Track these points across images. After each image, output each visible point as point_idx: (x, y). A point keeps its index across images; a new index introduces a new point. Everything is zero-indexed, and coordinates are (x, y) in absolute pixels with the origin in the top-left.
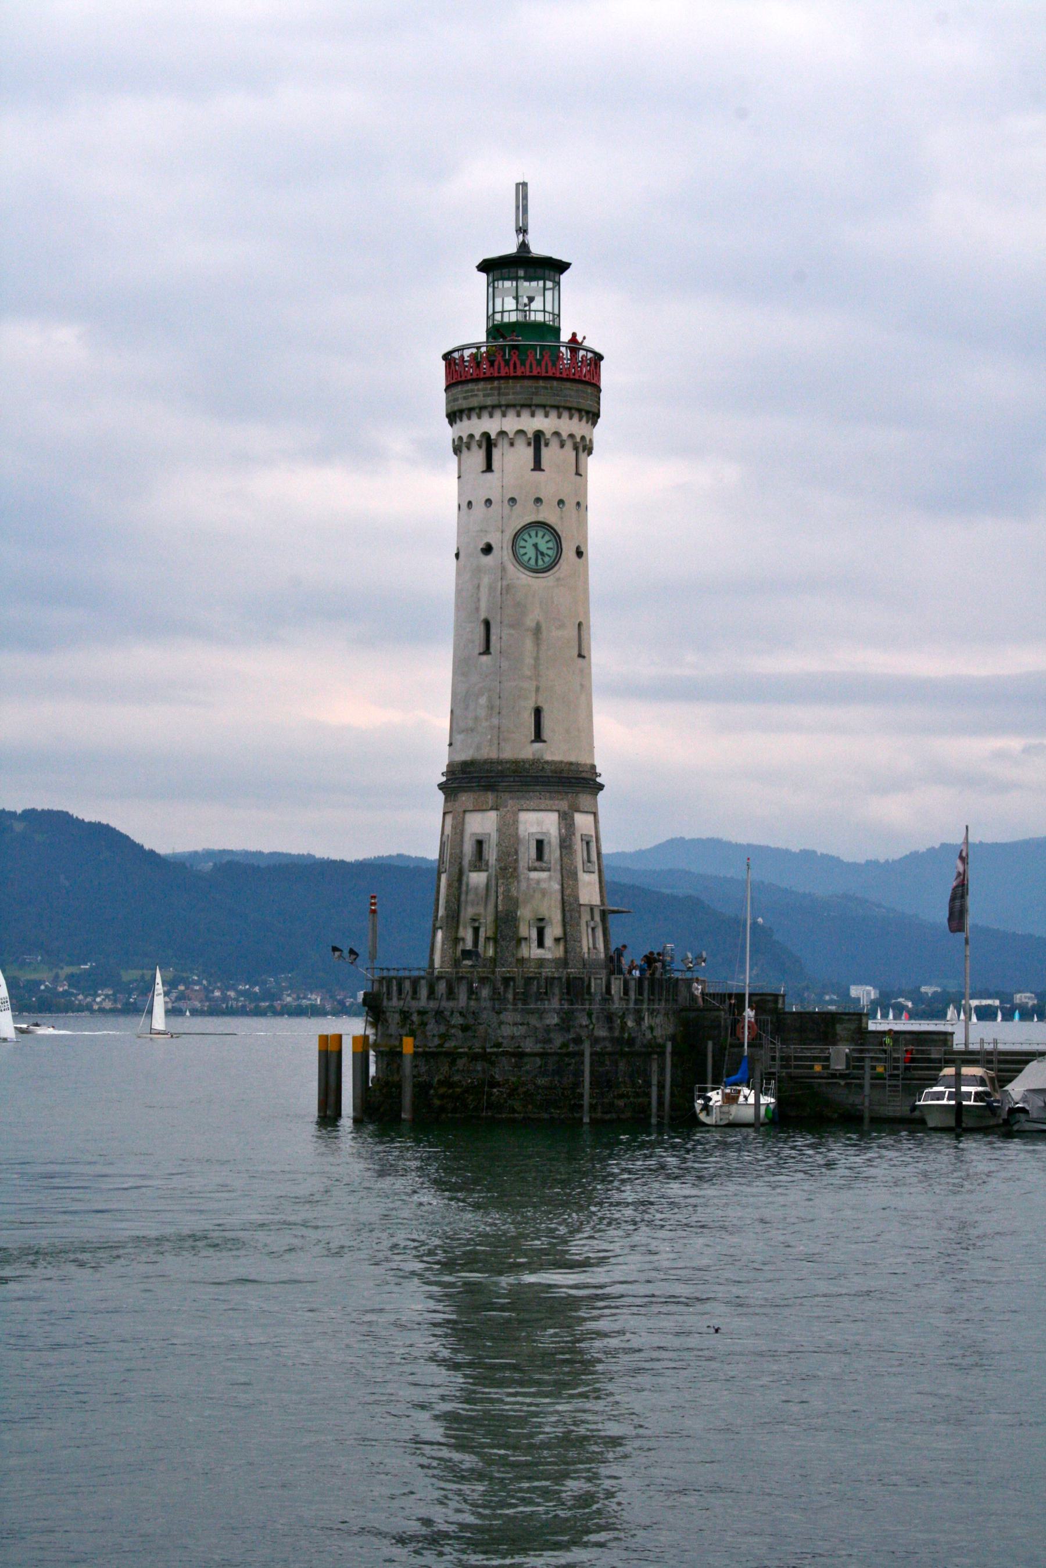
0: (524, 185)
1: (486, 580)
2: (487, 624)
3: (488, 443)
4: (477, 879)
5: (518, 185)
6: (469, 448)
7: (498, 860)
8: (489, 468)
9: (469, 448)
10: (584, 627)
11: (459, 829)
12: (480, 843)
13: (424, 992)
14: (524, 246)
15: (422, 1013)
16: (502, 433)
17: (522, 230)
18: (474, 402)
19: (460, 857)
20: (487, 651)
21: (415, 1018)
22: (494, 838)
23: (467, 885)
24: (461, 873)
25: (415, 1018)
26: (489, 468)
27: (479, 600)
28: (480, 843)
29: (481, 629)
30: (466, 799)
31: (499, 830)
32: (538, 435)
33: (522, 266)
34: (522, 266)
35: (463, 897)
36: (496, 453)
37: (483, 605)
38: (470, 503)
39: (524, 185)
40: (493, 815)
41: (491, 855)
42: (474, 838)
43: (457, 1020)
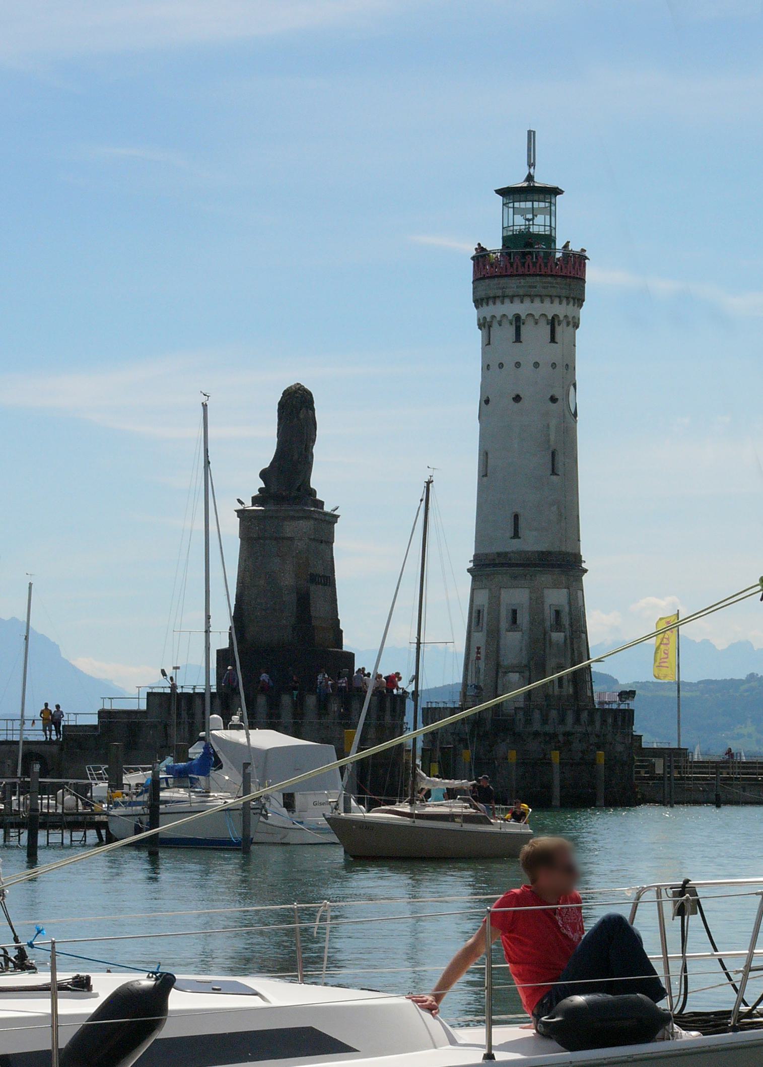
0: (534, 132)
1: (553, 423)
2: (553, 454)
3: (553, 323)
4: (557, 637)
5: (529, 132)
6: (536, 323)
7: (571, 625)
8: (553, 340)
9: (536, 323)
10: (560, 458)
11: (537, 602)
12: (558, 613)
13: (570, 719)
14: (530, 178)
15: (567, 734)
16: (566, 316)
17: (531, 165)
18: (553, 292)
19: (543, 620)
20: (554, 472)
21: (561, 738)
22: (567, 609)
23: (550, 640)
24: (545, 633)
25: (561, 738)
26: (553, 340)
27: (549, 435)
28: (558, 613)
29: (549, 457)
30: (545, 578)
31: (570, 603)
32: (518, 318)
33: (531, 193)
34: (531, 193)
35: (547, 650)
36: (559, 329)
37: (552, 438)
38: (536, 365)
39: (534, 132)
40: (565, 591)
41: (566, 621)
42: (553, 608)
43: (593, 740)
